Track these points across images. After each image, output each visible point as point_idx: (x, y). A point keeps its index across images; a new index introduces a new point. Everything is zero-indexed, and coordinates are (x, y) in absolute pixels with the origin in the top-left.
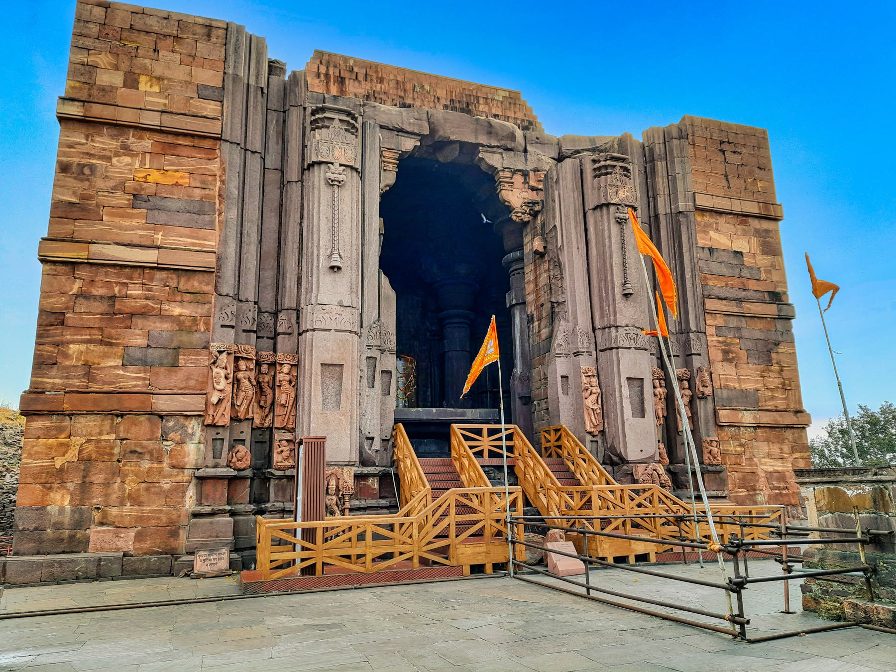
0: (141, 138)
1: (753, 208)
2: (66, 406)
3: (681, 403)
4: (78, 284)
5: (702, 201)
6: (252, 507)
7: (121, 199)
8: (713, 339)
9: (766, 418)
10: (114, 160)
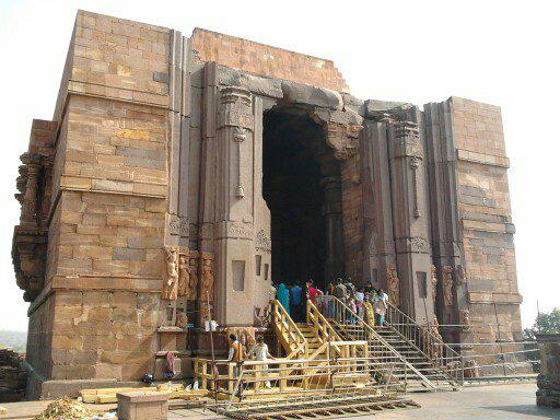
0: (120, 108)
1: (491, 160)
2: (80, 286)
3: (448, 290)
4: (84, 205)
6: (189, 352)
7: (110, 150)
8: (467, 246)
10: (104, 123)
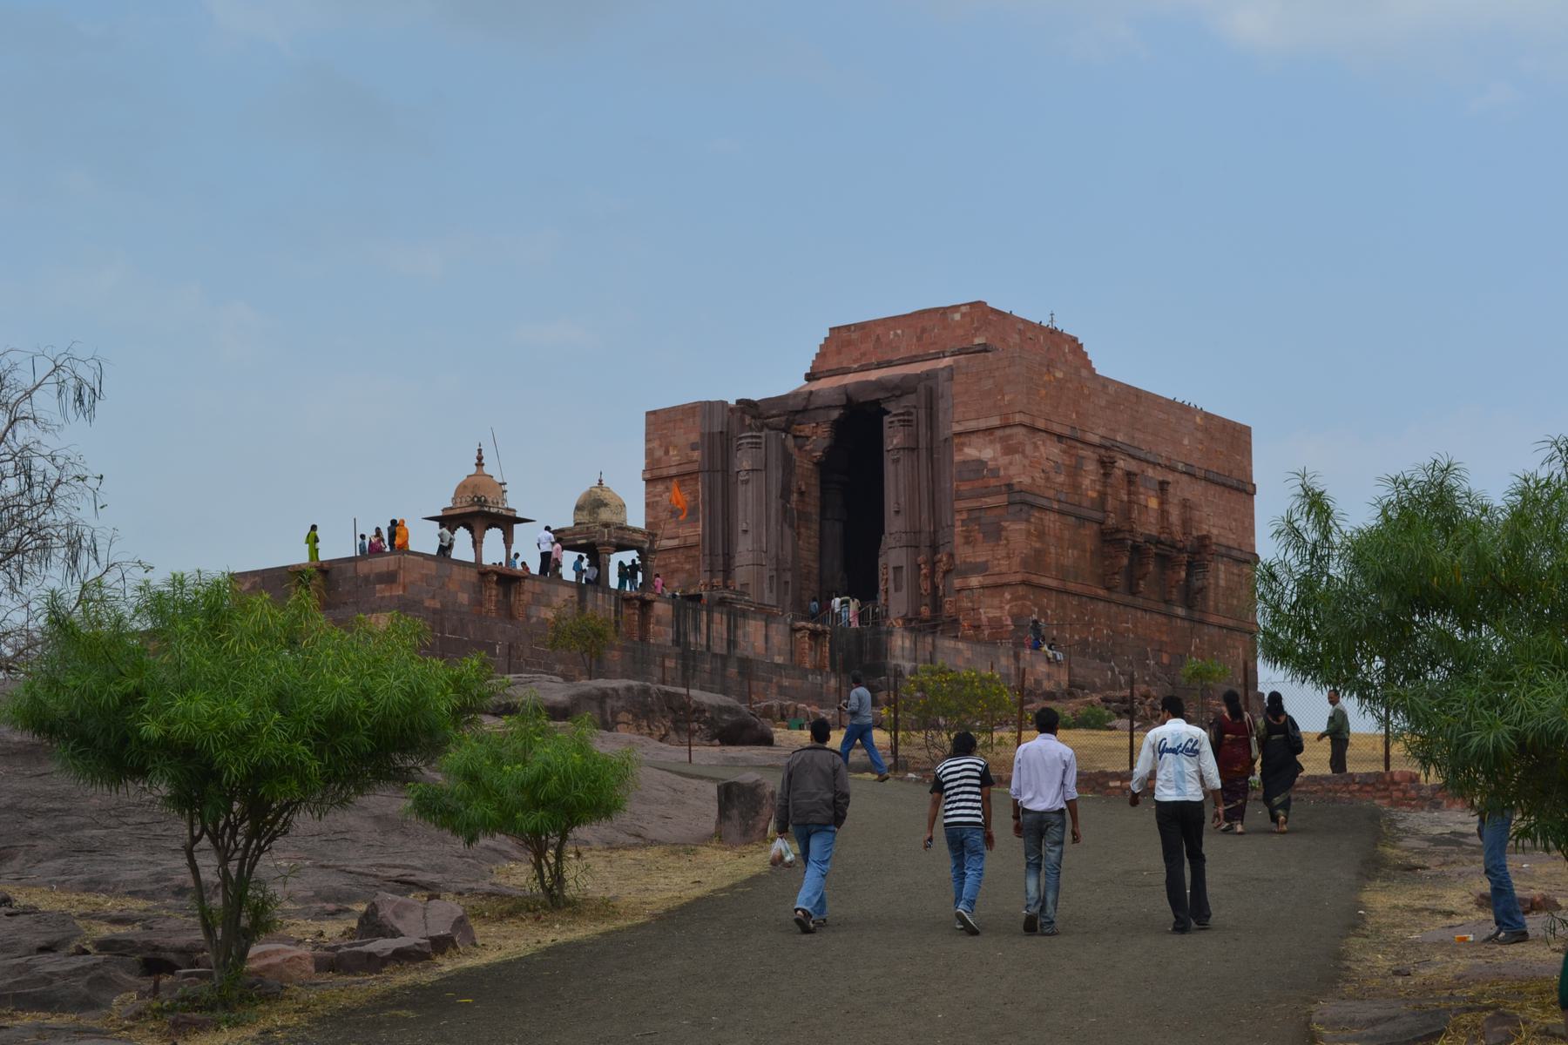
5: (957, 428)
8: (958, 529)
9: (989, 581)
